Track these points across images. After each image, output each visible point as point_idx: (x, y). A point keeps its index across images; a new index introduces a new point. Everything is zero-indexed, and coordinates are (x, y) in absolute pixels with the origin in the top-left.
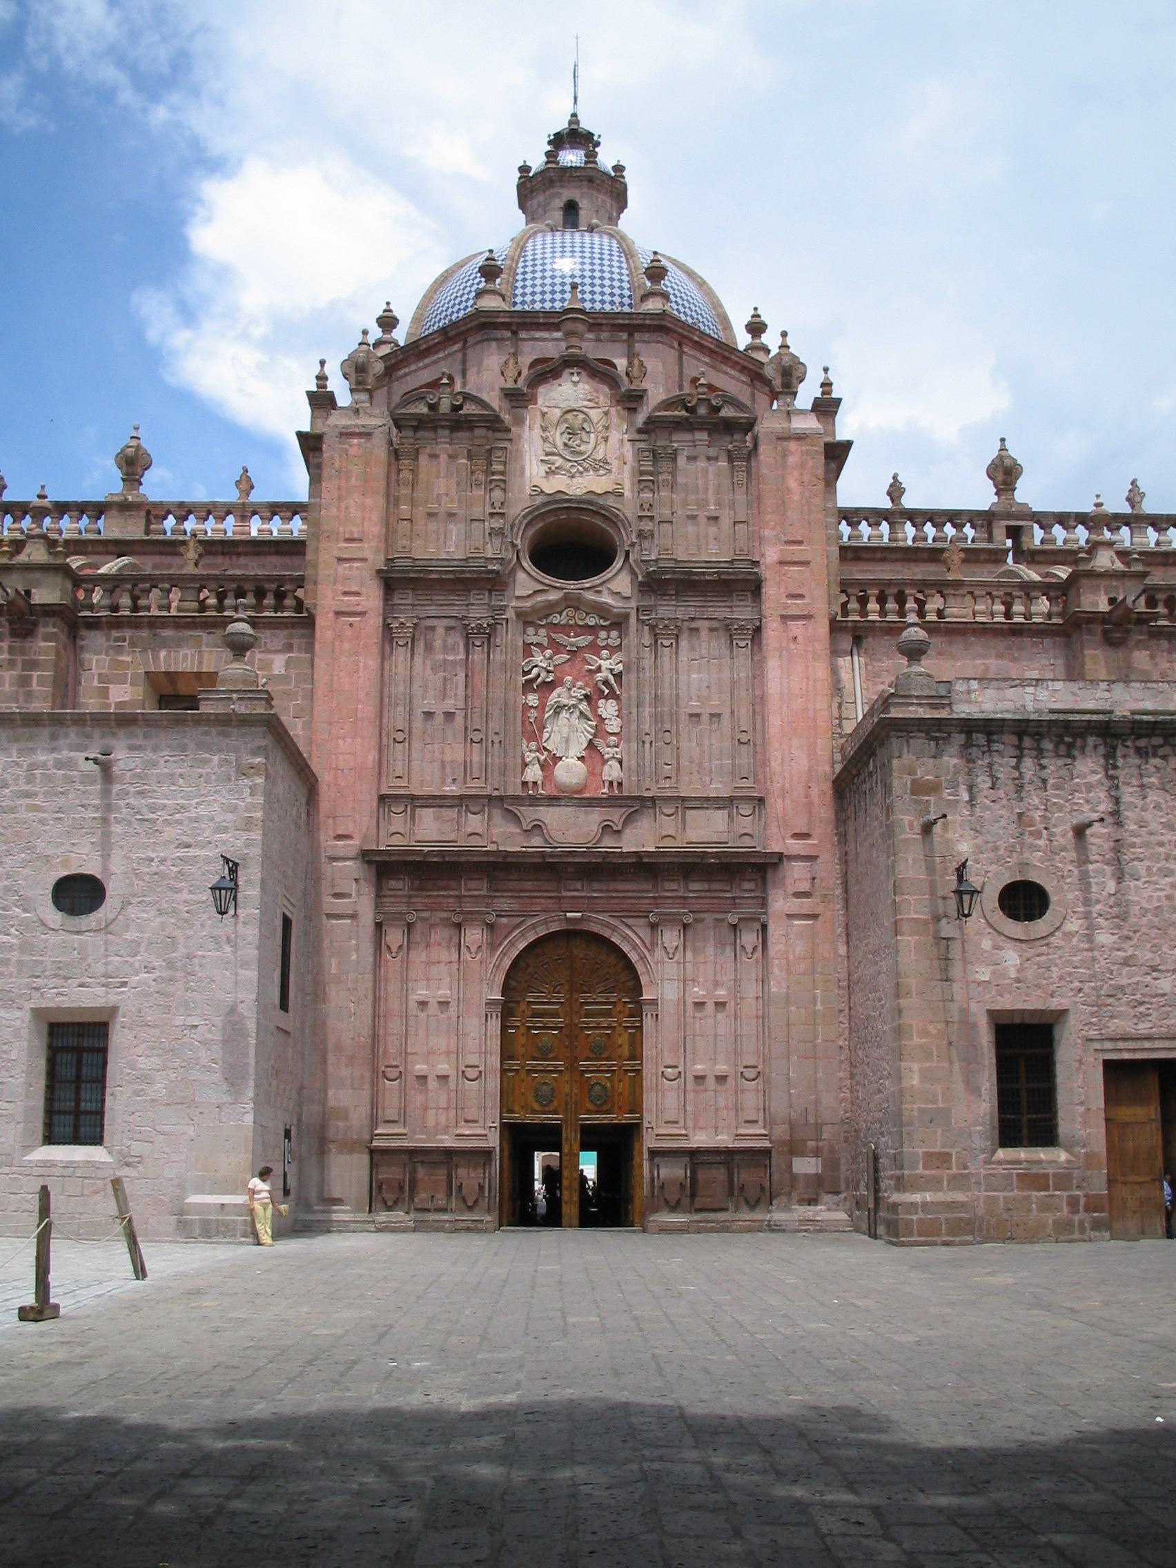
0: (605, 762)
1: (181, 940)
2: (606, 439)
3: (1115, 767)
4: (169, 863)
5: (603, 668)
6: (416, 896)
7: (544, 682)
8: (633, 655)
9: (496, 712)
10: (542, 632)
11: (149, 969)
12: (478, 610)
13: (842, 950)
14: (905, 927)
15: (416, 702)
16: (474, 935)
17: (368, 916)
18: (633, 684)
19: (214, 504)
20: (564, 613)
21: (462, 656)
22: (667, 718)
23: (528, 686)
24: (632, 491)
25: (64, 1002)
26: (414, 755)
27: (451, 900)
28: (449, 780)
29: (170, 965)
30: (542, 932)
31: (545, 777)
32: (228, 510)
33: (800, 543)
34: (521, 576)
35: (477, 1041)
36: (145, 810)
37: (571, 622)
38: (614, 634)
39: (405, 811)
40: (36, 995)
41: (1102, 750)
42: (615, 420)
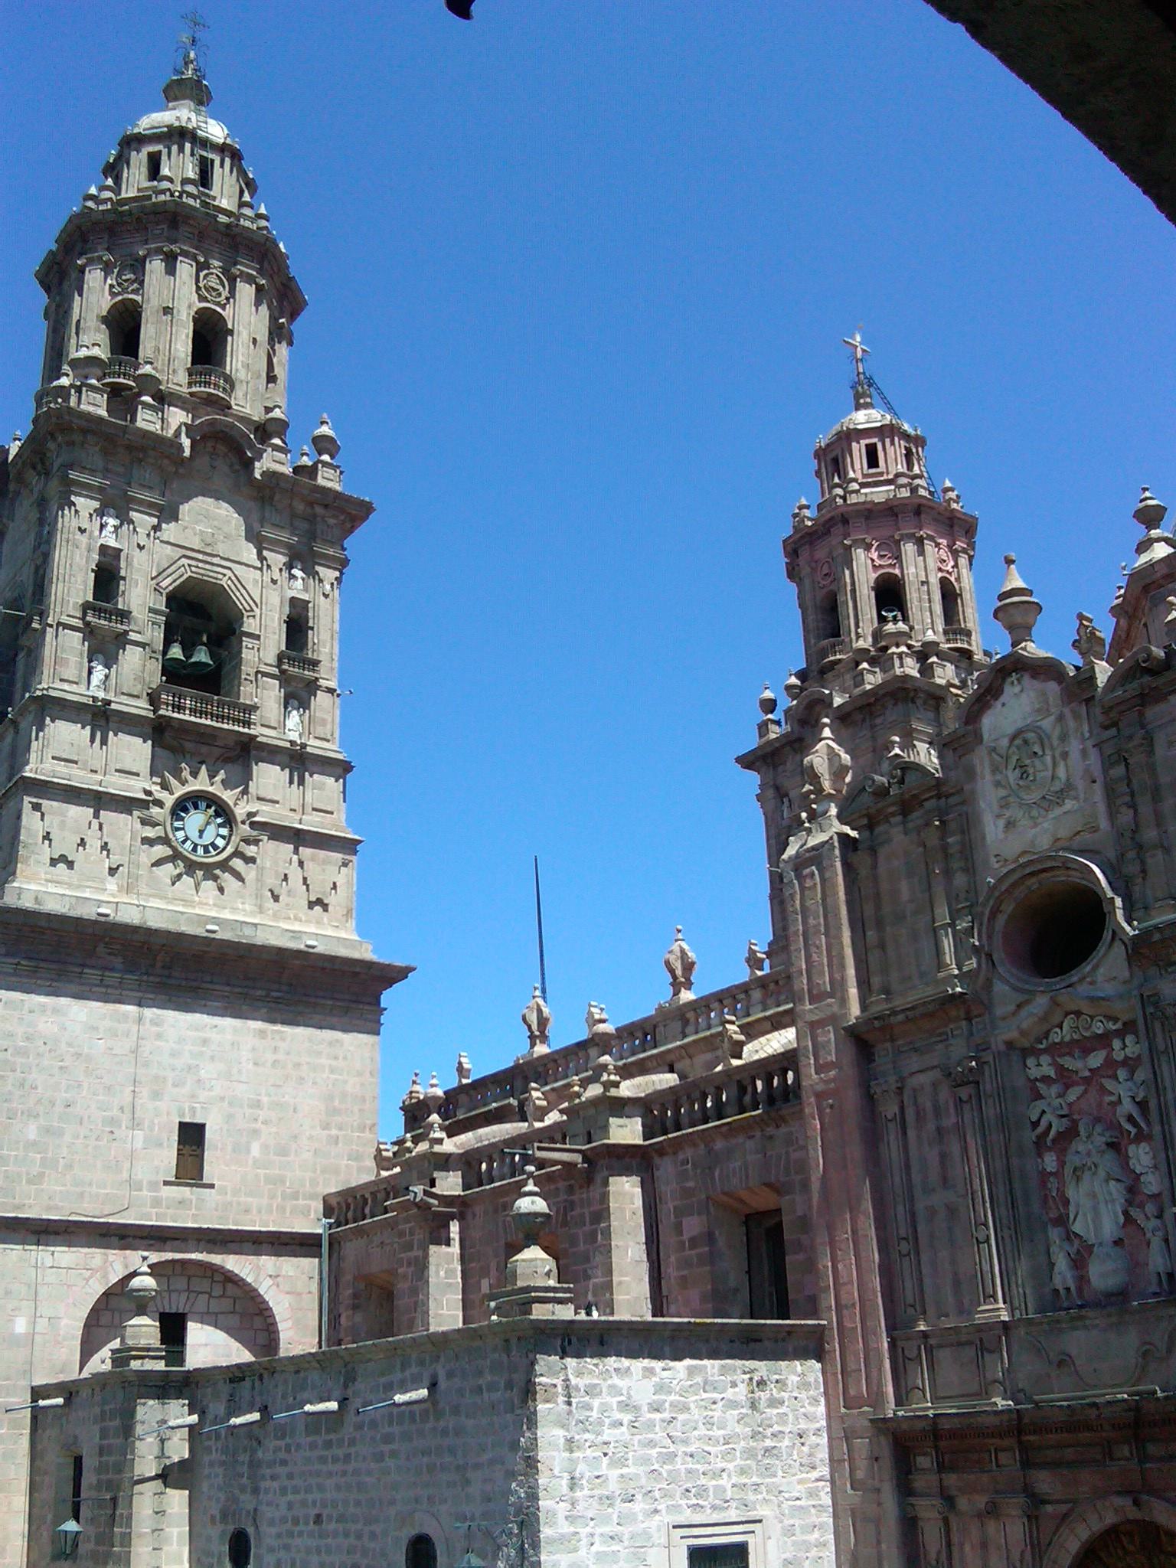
2: (1065, 755)
7: (1059, 1133)
10: (1045, 1059)
20: (1065, 1026)
23: (1040, 1145)
26: (924, 1271)
38: (1129, 1039)
42: (1071, 724)
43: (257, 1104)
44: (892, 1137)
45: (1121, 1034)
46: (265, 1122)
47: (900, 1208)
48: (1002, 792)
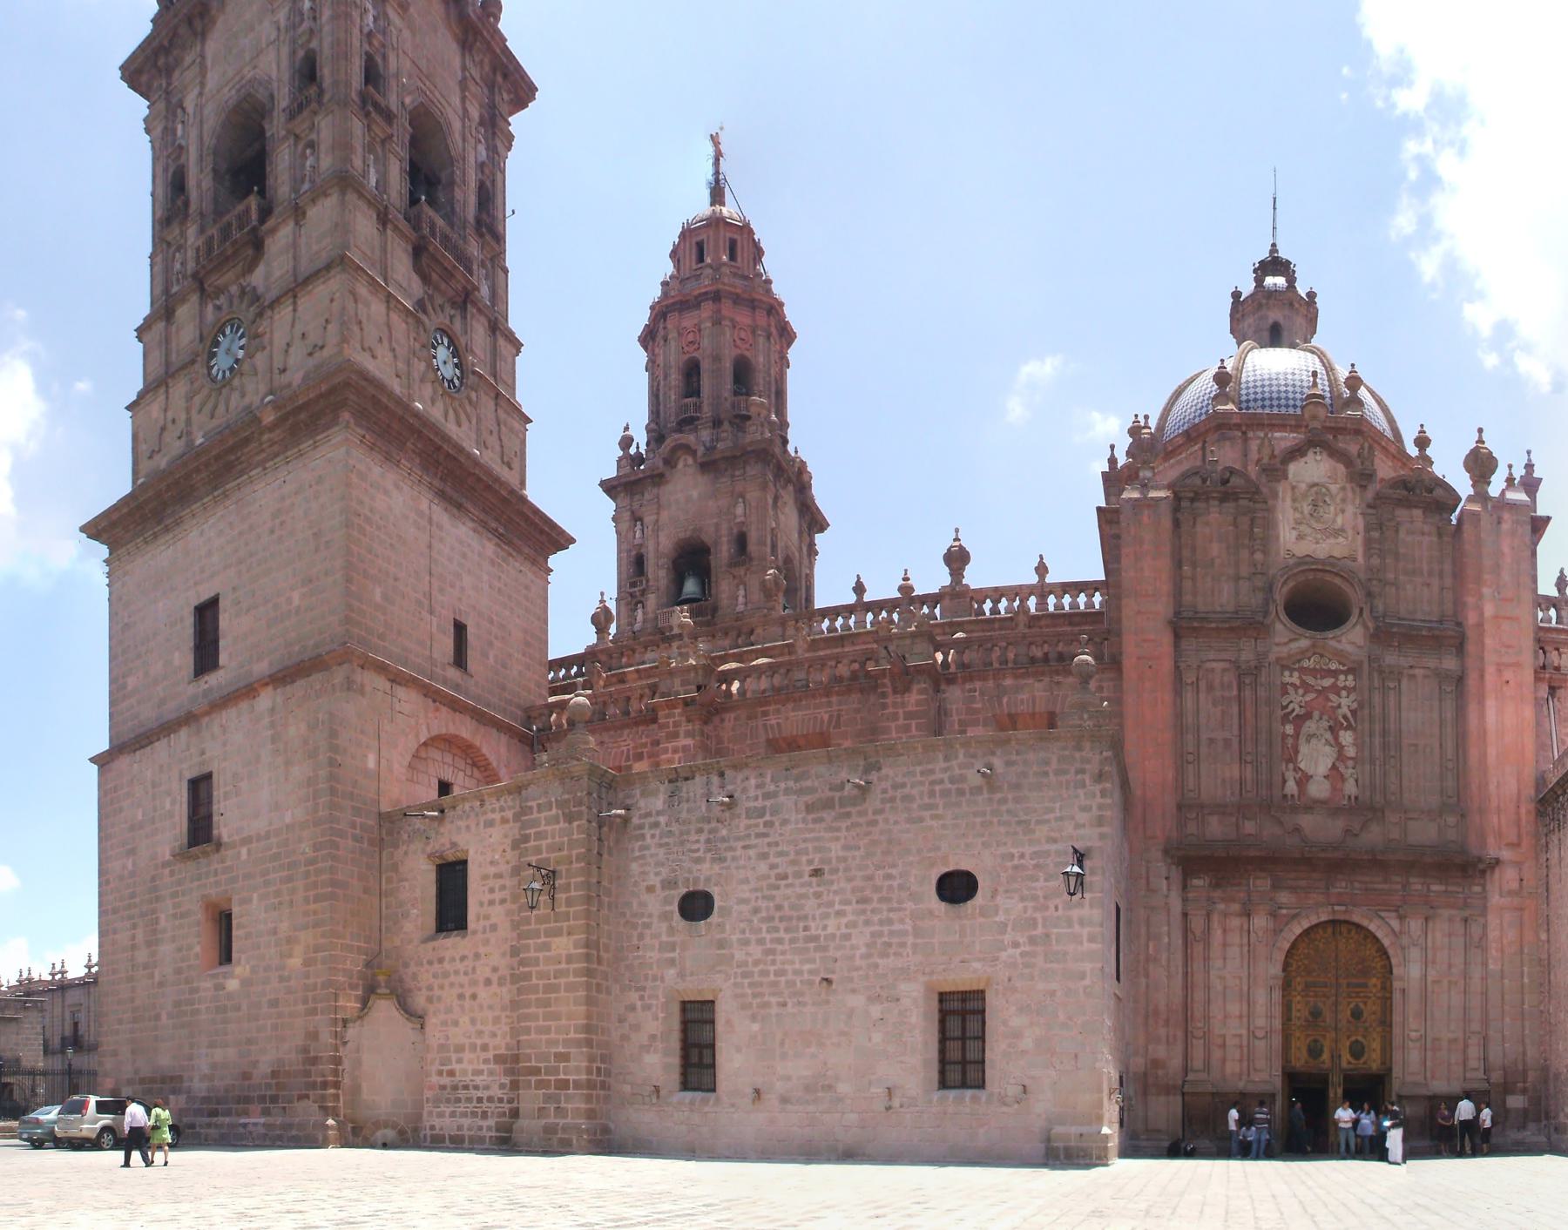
17: (1176, 906)
28: (1229, 793)
39: (1197, 817)
43: (492, 622)
46: (496, 638)
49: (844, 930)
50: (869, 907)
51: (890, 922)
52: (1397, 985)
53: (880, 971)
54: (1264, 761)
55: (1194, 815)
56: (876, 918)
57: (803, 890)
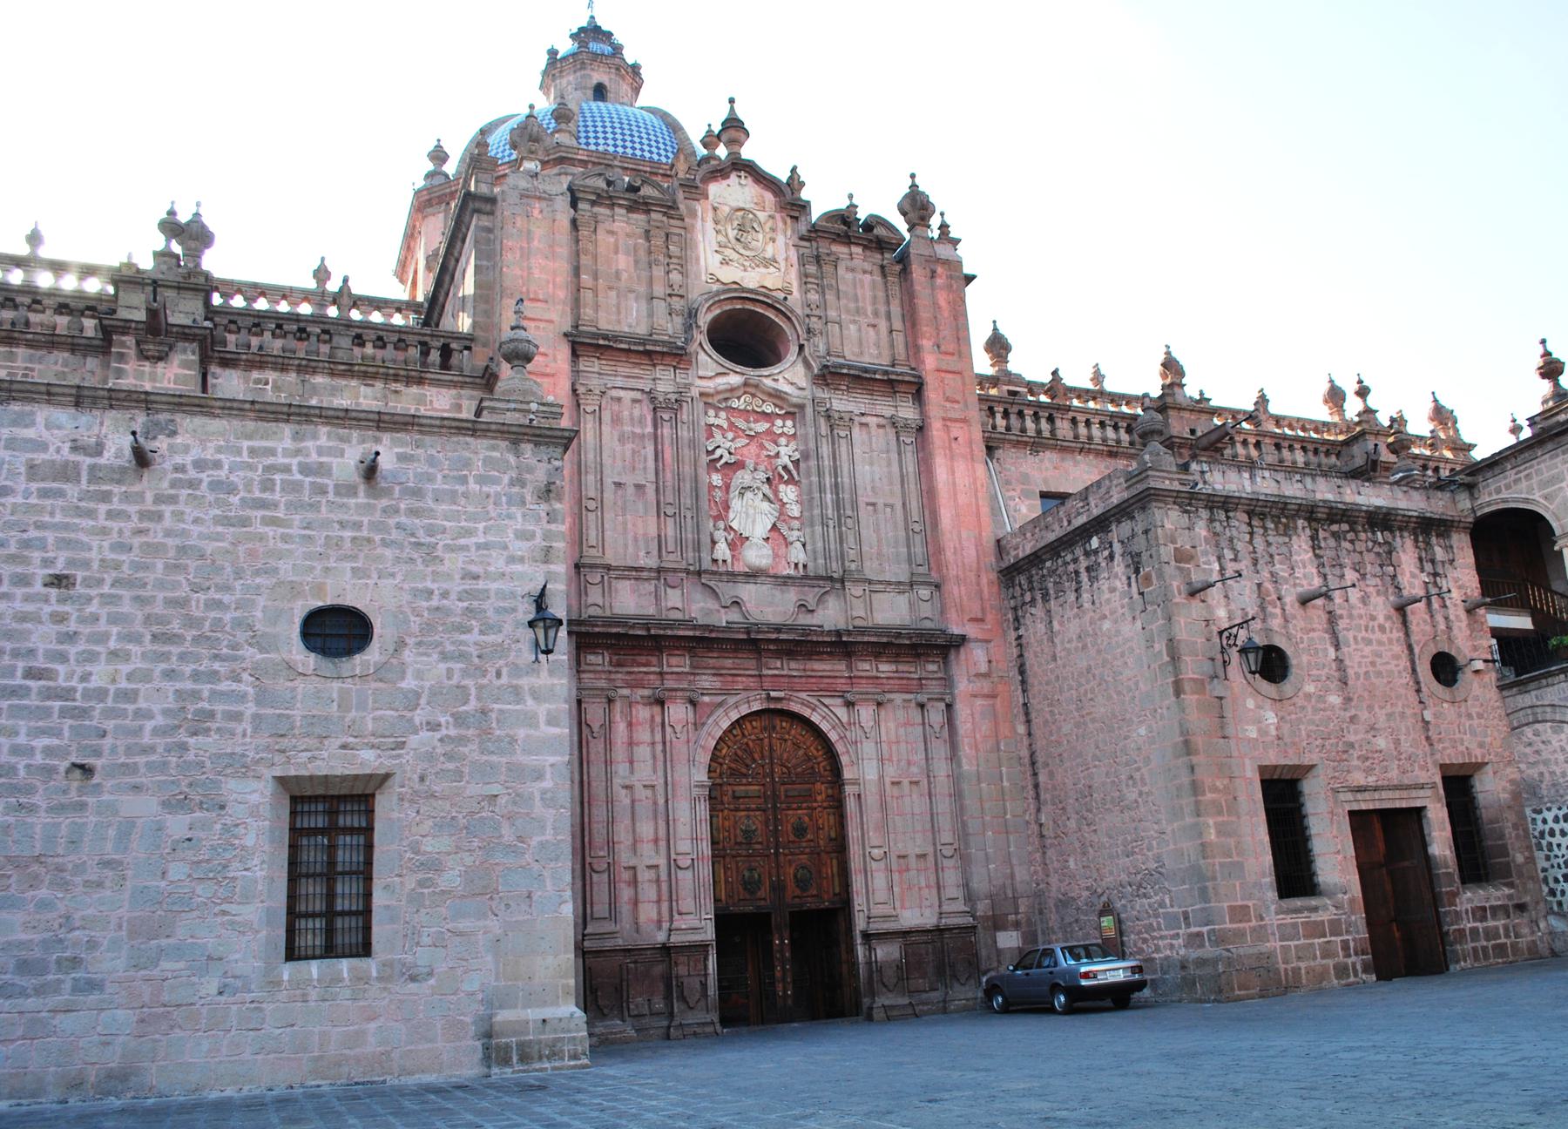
0: (788, 544)
1: (473, 691)
2: (773, 240)
3: (1320, 548)
4: (453, 596)
5: (782, 453)
6: (617, 672)
8: (812, 445)
9: (687, 487)
10: (723, 414)
11: (434, 726)
12: (665, 381)
13: (1021, 729)
14: (1187, 687)
15: (607, 471)
16: (678, 712)
18: (814, 470)
19: (291, 289)
21: (649, 429)
22: (848, 506)
24: (800, 291)
25: (321, 769)
26: (606, 526)
27: (652, 677)
28: (642, 554)
29: (459, 720)
30: (745, 710)
31: (733, 556)
32: (306, 296)
33: (953, 354)
34: (702, 356)
35: (688, 826)
36: (421, 533)
37: (749, 408)
38: (789, 423)
39: (602, 581)
40: (278, 758)
41: (1308, 532)
42: (780, 225)
44: (589, 425)
45: (783, 417)
47: (591, 478)
48: (721, 238)
49: (124, 684)
50: (175, 650)
51: (214, 676)
52: (849, 790)
53: (190, 756)
54: (689, 515)
55: (599, 579)
56: (188, 669)
57: (30, 607)
